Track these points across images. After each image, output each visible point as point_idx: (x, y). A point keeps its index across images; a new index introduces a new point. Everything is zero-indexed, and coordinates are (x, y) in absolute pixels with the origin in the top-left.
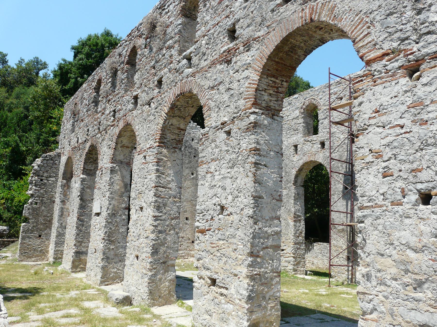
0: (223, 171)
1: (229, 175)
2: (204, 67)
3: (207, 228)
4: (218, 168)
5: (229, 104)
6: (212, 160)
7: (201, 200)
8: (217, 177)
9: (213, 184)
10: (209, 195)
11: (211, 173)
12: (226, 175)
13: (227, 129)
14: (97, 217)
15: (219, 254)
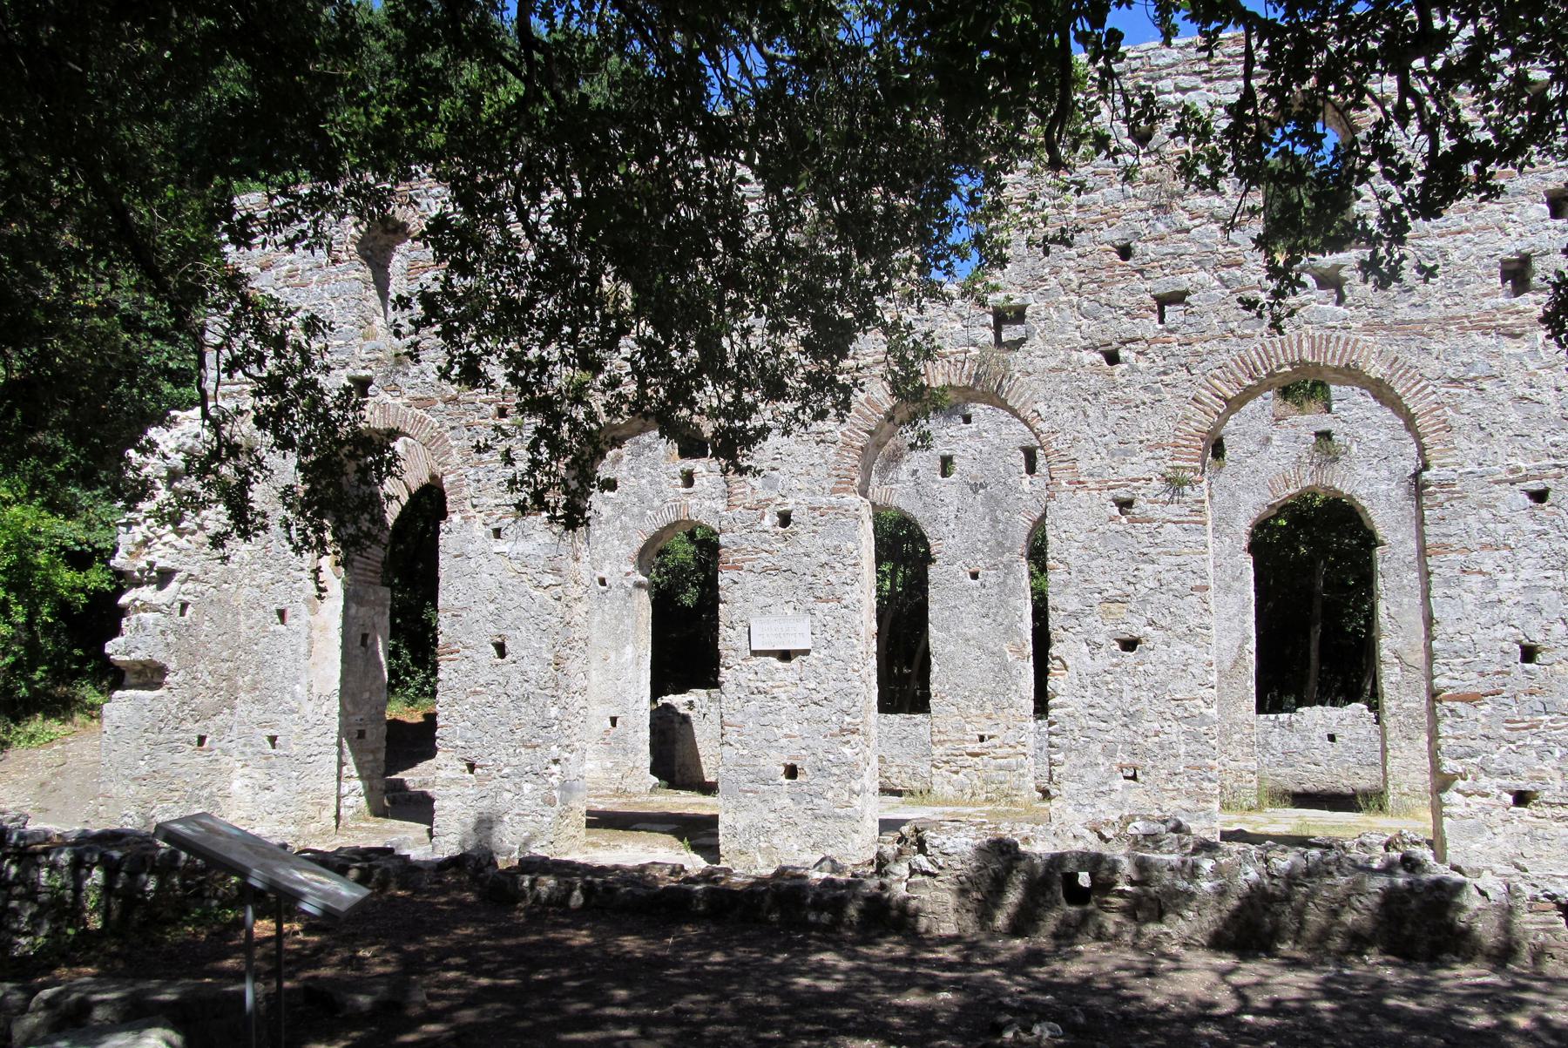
0: (1523, 574)
1: (1551, 583)
2: (1411, 322)
3: (1482, 691)
4: (1508, 567)
5: (1525, 431)
6: (1484, 547)
7: (1450, 630)
8: (1504, 585)
9: (1493, 596)
10: (1482, 620)
11: (1480, 572)
12: (1542, 583)
13: (1534, 485)
14: (779, 664)
15: (1539, 742)
